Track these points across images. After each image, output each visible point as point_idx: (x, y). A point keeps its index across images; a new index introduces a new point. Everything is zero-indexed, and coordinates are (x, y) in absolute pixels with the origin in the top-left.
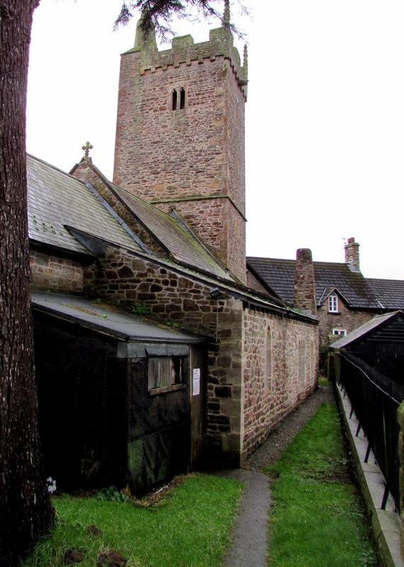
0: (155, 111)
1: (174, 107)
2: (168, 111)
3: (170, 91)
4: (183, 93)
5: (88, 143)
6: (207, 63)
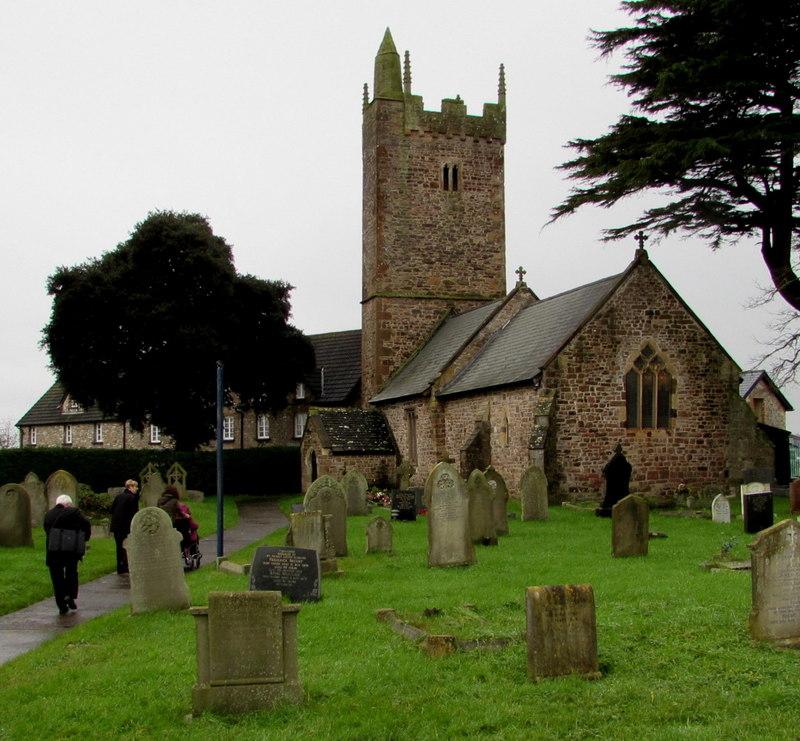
1: (446, 187)
2: (440, 189)
3: (443, 166)
4: (455, 171)
5: (521, 268)
6: (482, 143)
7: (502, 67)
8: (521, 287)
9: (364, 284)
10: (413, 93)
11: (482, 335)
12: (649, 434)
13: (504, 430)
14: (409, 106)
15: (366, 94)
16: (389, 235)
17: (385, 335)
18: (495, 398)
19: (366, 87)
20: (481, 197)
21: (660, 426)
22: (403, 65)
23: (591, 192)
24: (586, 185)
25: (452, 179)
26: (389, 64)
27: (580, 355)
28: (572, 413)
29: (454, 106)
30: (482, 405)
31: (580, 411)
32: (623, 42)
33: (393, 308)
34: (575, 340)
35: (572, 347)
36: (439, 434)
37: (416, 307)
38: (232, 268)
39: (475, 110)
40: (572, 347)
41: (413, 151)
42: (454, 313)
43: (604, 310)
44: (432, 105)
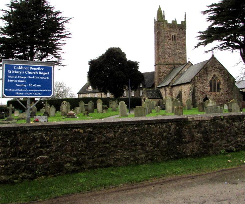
0: (168, 40)
1: (173, 40)
4: (175, 36)
6: (181, 30)
7: (185, 13)
8: (189, 62)
9: (155, 61)
10: (165, 19)
11: (180, 73)
12: (215, 93)
13: (184, 92)
14: (164, 23)
15: (155, 19)
16: (160, 51)
17: (159, 73)
18: (183, 86)
19: (155, 18)
20: (181, 42)
21: (217, 91)
22: (163, 13)
23: (202, 43)
24: (201, 41)
25: (174, 38)
26: (160, 13)
27: (200, 77)
28: (198, 89)
29: (174, 22)
30: (180, 88)
31: (200, 88)
32: (207, 13)
33: (161, 67)
34: (199, 74)
35: (198, 75)
36: (171, 94)
37: (166, 66)
38: (126, 59)
39: (179, 22)
40: (198, 75)
41: (166, 33)
42: (175, 68)
43: (205, 67)
44: (170, 22)
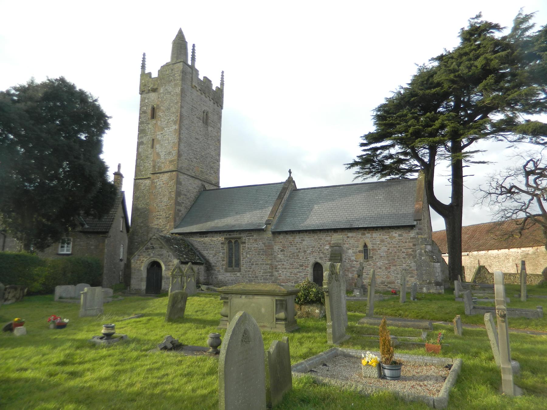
6: (216, 105)
18: (350, 234)
29: (207, 82)
